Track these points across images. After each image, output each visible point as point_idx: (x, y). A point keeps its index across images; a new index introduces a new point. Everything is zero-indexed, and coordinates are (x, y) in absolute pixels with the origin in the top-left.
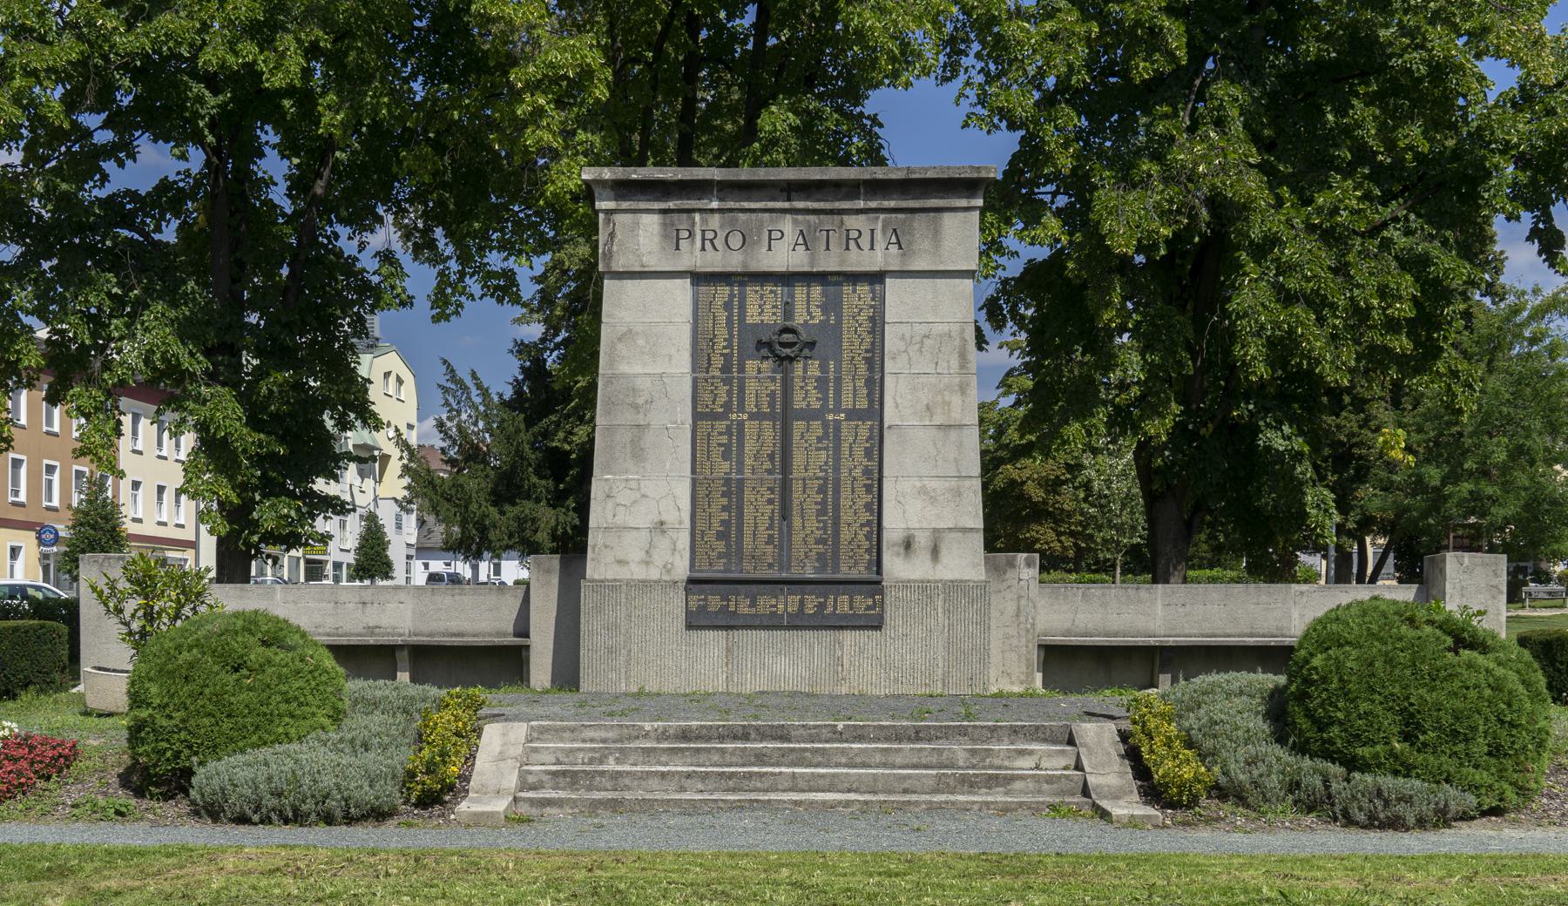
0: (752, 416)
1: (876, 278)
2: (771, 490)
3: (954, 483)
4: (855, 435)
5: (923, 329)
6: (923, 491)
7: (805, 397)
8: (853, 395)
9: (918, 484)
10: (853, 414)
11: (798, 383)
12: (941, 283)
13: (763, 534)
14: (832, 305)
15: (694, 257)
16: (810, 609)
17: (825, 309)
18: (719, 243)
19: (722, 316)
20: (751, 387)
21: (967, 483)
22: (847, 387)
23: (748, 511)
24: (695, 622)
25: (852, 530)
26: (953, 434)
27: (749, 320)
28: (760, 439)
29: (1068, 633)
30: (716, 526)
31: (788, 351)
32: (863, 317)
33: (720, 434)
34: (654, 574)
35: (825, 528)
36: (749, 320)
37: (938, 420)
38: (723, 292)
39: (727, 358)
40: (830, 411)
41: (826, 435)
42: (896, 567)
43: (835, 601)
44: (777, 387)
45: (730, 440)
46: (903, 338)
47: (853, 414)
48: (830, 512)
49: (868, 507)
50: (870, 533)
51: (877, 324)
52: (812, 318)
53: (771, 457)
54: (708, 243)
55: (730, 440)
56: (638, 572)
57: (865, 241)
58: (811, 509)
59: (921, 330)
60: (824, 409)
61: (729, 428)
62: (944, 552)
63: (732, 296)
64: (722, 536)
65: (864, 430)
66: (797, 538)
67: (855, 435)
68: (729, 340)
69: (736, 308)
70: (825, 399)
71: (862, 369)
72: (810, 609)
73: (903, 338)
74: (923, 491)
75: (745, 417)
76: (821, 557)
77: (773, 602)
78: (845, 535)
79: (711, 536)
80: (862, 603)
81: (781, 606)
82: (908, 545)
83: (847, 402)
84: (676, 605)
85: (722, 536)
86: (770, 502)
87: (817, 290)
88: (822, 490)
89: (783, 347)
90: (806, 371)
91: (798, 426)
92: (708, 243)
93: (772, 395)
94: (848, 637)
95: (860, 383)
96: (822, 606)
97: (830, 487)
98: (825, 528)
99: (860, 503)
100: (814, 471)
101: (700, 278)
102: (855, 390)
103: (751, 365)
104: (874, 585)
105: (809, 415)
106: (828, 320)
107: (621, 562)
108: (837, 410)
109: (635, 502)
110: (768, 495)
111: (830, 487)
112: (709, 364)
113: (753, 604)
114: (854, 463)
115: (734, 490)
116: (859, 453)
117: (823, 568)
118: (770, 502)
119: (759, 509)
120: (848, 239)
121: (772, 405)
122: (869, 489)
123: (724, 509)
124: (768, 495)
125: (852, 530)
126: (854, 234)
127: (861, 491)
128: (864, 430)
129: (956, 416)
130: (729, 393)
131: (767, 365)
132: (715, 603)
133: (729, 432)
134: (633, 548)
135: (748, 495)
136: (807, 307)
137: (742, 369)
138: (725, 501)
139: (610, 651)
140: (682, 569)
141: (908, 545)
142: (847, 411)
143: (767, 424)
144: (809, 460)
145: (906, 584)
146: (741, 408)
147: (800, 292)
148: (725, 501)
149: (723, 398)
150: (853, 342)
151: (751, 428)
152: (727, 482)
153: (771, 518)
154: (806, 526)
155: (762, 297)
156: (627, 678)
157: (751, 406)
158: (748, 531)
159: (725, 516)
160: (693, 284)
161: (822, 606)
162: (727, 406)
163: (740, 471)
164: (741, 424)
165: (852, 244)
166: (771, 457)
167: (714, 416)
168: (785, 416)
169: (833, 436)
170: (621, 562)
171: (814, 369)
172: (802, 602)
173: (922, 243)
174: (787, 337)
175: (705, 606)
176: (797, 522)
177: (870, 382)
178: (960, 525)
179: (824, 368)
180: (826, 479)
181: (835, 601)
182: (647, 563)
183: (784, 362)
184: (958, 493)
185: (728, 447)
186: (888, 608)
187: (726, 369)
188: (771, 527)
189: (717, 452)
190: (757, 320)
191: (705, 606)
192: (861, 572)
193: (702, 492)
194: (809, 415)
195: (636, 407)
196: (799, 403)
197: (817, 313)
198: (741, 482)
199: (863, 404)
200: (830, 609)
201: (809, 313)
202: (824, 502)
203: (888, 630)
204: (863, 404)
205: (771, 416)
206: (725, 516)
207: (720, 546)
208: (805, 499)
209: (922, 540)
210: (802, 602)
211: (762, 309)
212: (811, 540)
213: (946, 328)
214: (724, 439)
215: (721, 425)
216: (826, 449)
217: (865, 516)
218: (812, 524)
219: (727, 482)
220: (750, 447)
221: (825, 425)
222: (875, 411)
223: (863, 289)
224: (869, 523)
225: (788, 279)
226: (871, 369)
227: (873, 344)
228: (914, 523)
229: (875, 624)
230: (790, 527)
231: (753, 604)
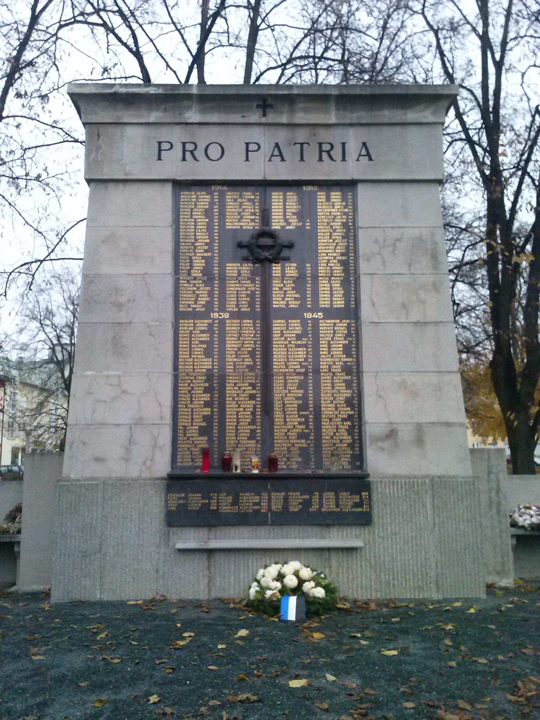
2: (253, 386)
3: (434, 379)
5: (395, 234)
6: (403, 385)
8: (330, 294)
9: (398, 379)
10: (331, 313)
11: (276, 284)
12: (411, 191)
13: (245, 430)
14: (307, 212)
15: (173, 167)
16: (295, 507)
17: (300, 216)
18: (200, 153)
19: (202, 221)
20: (232, 287)
21: (447, 377)
22: (324, 285)
24: (175, 519)
25: (334, 430)
26: (430, 330)
27: (229, 226)
28: (241, 338)
30: (199, 422)
31: (266, 254)
32: (337, 224)
33: (202, 332)
34: (134, 471)
35: (306, 423)
36: (229, 226)
37: (415, 317)
38: (204, 199)
40: (308, 310)
42: (379, 462)
43: (321, 498)
44: (257, 287)
45: (212, 337)
46: (376, 242)
47: (331, 313)
49: (349, 402)
50: (352, 427)
51: (351, 231)
52: (289, 224)
53: (252, 354)
54: (188, 154)
55: (212, 337)
56: (115, 469)
57: (337, 153)
59: (394, 234)
60: (303, 308)
61: (210, 326)
63: (212, 203)
64: (202, 431)
65: (342, 326)
66: (279, 432)
67: (332, 332)
68: (210, 245)
69: (216, 215)
70: (303, 299)
72: (295, 507)
73: (376, 242)
74: (403, 385)
75: (227, 316)
76: (303, 452)
77: (256, 499)
78: (327, 429)
79: (193, 431)
80: (348, 500)
81: (264, 504)
83: (324, 302)
84: (155, 504)
85: (202, 431)
86: (252, 397)
87: (292, 197)
88: (302, 385)
90: (283, 273)
91: (278, 325)
92: (188, 154)
93: (252, 295)
95: (337, 285)
96: (307, 504)
98: (306, 423)
99: (341, 399)
100: (294, 366)
101: (180, 185)
102: (331, 291)
103: (232, 268)
105: (287, 314)
106: (304, 226)
107: (99, 460)
108: (315, 308)
109: (116, 398)
110: (250, 390)
111: (312, 373)
112: (191, 267)
113: (236, 502)
114: (332, 356)
115: (216, 383)
117: (306, 462)
118: (252, 397)
119: (240, 406)
120: (321, 151)
121: (252, 304)
122: (348, 385)
123: (207, 404)
124: (250, 390)
125: (334, 430)
126: (326, 147)
128: (342, 326)
129: (432, 315)
130: (211, 294)
131: (246, 268)
132: (196, 501)
133: (210, 330)
134: (111, 445)
135: (230, 390)
136: (284, 213)
138: (206, 397)
139: (85, 555)
140: (162, 466)
142: (324, 310)
143: (248, 322)
146: (222, 308)
148: (206, 397)
149: (204, 299)
150: (329, 249)
151: (232, 326)
153: (253, 413)
155: (241, 204)
156: (102, 585)
157: (231, 306)
158: (230, 425)
159: (207, 411)
160: (173, 188)
161: (307, 504)
162: (209, 306)
164: (222, 322)
165: (325, 155)
166: (252, 354)
167: (194, 315)
170: (99, 460)
171: (291, 270)
172: (286, 499)
175: (185, 505)
176: (278, 416)
177: (345, 283)
178: (443, 419)
179: (301, 269)
180: (306, 374)
181: (321, 498)
182: (127, 460)
184: (438, 388)
185: (209, 344)
186: (375, 505)
187: (207, 272)
188: (253, 422)
189: (199, 350)
190: (237, 226)
191: (185, 505)
193: (183, 388)
194: (287, 314)
195: (119, 306)
196: (277, 302)
197: (294, 222)
198: (223, 378)
199: (339, 303)
200: (314, 508)
201: (286, 220)
202: (305, 397)
204: (339, 303)
205: (250, 315)
206: (207, 411)
209: (406, 434)
210: (286, 499)
211: (242, 216)
212: (293, 434)
213: (417, 232)
214: (205, 337)
215: (203, 324)
216: (305, 346)
218: (294, 419)
220: (231, 344)
221: (304, 323)
222: (352, 312)
223: (336, 196)
224: (350, 418)
227: (347, 248)
228: (396, 418)
229: (363, 519)
230: (272, 422)
231: (236, 502)
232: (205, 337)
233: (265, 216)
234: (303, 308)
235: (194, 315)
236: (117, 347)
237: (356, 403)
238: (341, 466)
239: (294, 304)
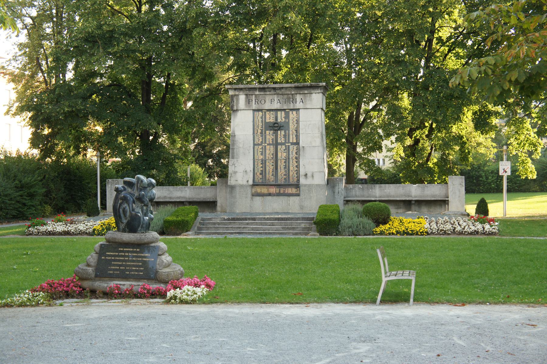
0: (268, 145)
4: (293, 149)
7: (281, 140)
8: (293, 139)
10: (293, 144)
11: (279, 136)
13: (271, 174)
14: (287, 117)
17: (285, 118)
19: (260, 120)
20: (268, 137)
22: (291, 137)
23: (267, 169)
28: (270, 150)
30: (260, 172)
32: (294, 120)
39: (262, 130)
41: (286, 149)
42: (302, 181)
44: (274, 137)
47: (293, 144)
48: (287, 167)
49: (297, 166)
51: (298, 122)
53: (273, 154)
58: (283, 167)
63: (263, 115)
64: (261, 174)
66: (279, 174)
68: (262, 126)
69: (264, 117)
70: (286, 140)
71: (295, 132)
78: (291, 173)
79: (258, 174)
82: (306, 175)
83: (291, 141)
84: (249, 191)
85: (261, 174)
88: (285, 162)
89: (276, 127)
90: (281, 133)
91: (279, 147)
95: (294, 136)
97: (287, 160)
99: (295, 166)
103: (267, 132)
104: (297, 186)
105: (282, 144)
108: (289, 142)
111: (287, 160)
114: (293, 155)
115: (264, 162)
116: (294, 153)
118: (273, 165)
119: (270, 167)
121: (273, 141)
122: (297, 162)
123: (262, 167)
128: (295, 147)
130: (262, 139)
131: (272, 132)
133: (262, 148)
135: (267, 164)
136: (281, 117)
137: (265, 133)
138: (261, 165)
141: (306, 175)
144: (282, 155)
145: (305, 185)
146: (265, 143)
147: (279, 113)
148: (261, 165)
149: (261, 140)
150: (292, 126)
151: (268, 147)
152: (262, 160)
154: (281, 172)
157: (267, 142)
158: (267, 172)
159: (262, 169)
161: (284, 191)
162: (262, 142)
163: (265, 158)
164: (265, 146)
166: (273, 154)
167: (258, 145)
168: (276, 144)
169: (288, 149)
171: (283, 133)
173: (308, 102)
174: (276, 125)
177: (296, 136)
179: (285, 132)
185: (262, 152)
187: (261, 133)
189: (259, 153)
190: (269, 121)
194: (282, 144)
196: (279, 141)
197: (284, 119)
199: (295, 141)
203: (301, 197)
204: (295, 141)
205: (273, 144)
206: (262, 169)
207: (261, 176)
208: (281, 164)
209: (309, 175)
211: (270, 118)
212: (283, 175)
214: (261, 150)
215: (260, 147)
217: (296, 169)
218: (283, 171)
219: (262, 160)
220: (268, 152)
221: (286, 146)
222: (297, 143)
223: (294, 112)
224: (297, 170)
226: (297, 132)
229: (298, 195)
232: (261, 150)
233: (276, 118)
234: (285, 142)
235: (258, 145)
237: (298, 166)
238: (293, 180)
239: (283, 141)
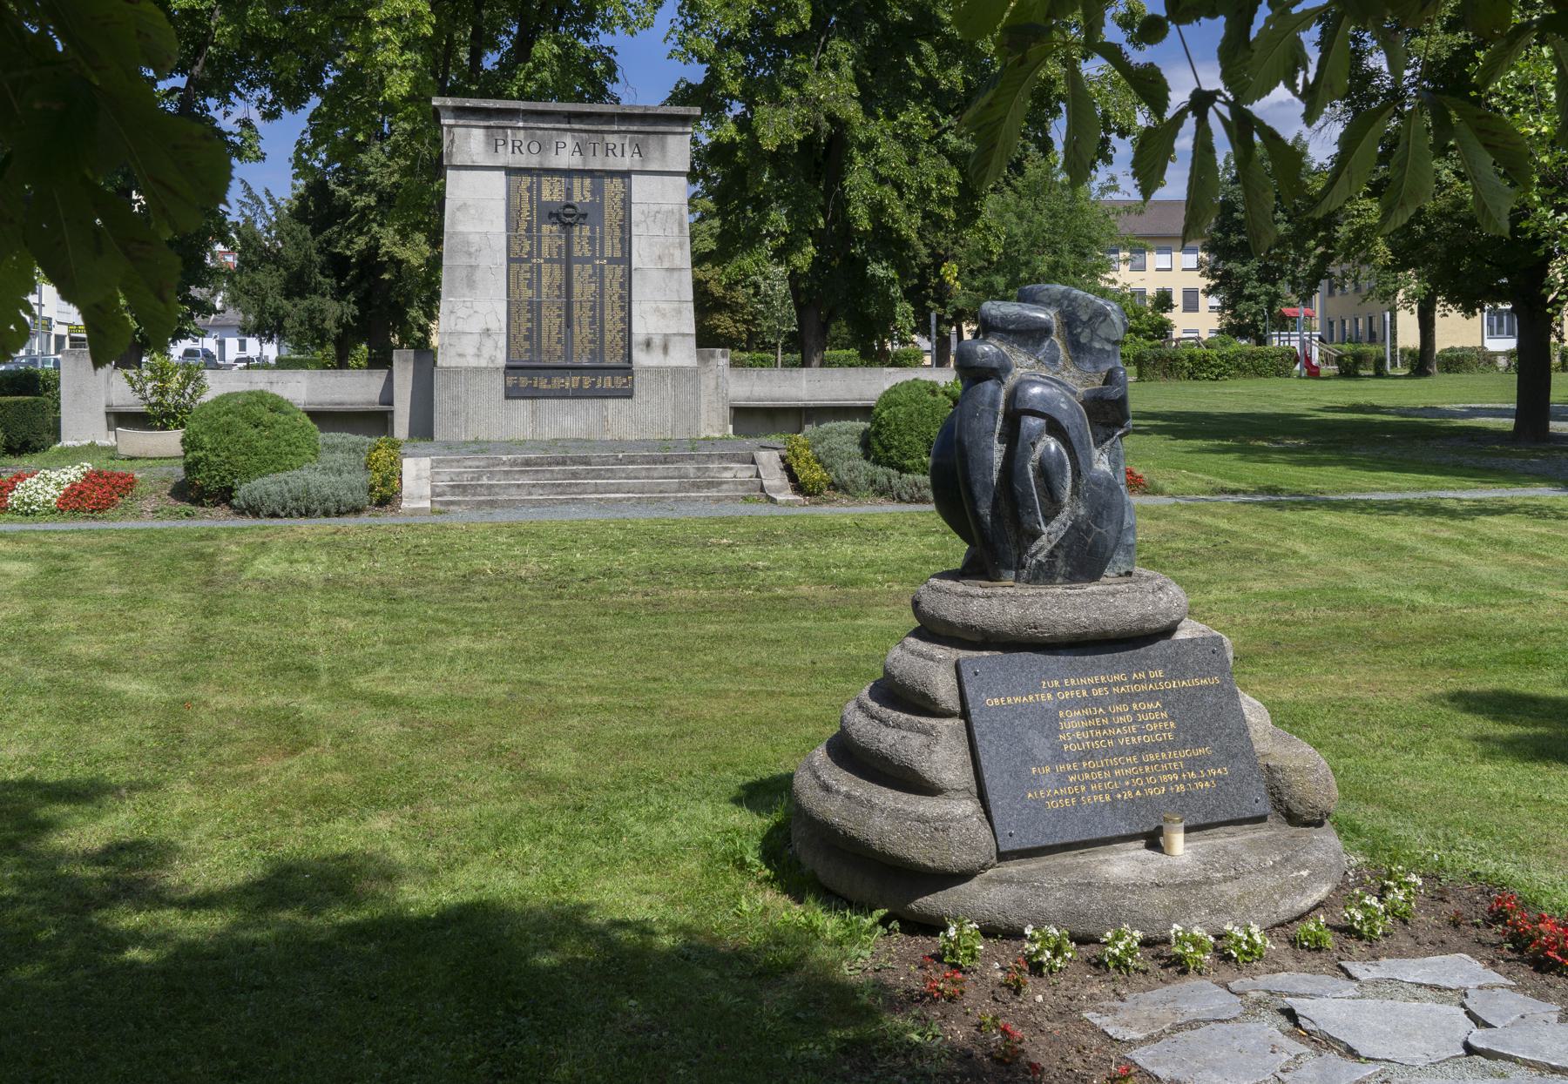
0: (546, 261)
1: (626, 175)
3: (676, 305)
4: (614, 274)
5: (656, 208)
6: (657, 310)
7: (581, 249)
8: (611, 248)
10: (612, 261)
11: (576, 240)
12: (666, 178)
14: (597, 191)
15: (506, 157)
16: (586, 385)
17: (593, 193)
20: (546, 243)
22: (608, 243)
23: (544, 323)
24: (511, 394)
26: (676, 274)
28: (551, 276)
29: (748, 399)
30: (524, 332)
34: (483, 363)
38: (527, 180)
39: (530, 223)
41: (594, 274)
42: (640, 358)
47: (612, 261)
48: (598, 322)
49: (622, 320)
51: (627, 203)
53: (559, 287)
56: (472, 362)
57: (618, 151)
58: (586, 321)
60: (593, 257)
62: (671, 348)
64: (527, 338)
65: (619, 271)
66: (577, 339)
67: (614, 274)
68: (531, 211)
70: (594, 251)
71: (618, 232)
72: (586, 385)
74: (657, 310)
76: (592, 352)
78: (608, 337)
79: (520, 338)
80: (620, 381)
82: (648, 344)
83: (608, 253)
84: (499, 383)
85: (527, 338)
87: (587, 181)
88: (593, 309)
89: (566, 217)
90: (581, 233)
91: (576, 268)
94: (611, 403)
95: (616, 241)
96: (594, 384)
97: (597, 307)
101: (510, 171)
103: (546, 228)
104: (627, 369)
105: (584, 260)
107: (461, 355)
108: (601, 258)
113: (549, 382)
114: (613, 289)
115: (535, 308)
116: (616, 286)
117: (593, 359)
119: (551, 321)
121: (559, 254)
122: (622, 308)
127: (617, 309)
129: (678, 263)
132: (524, 381)
133: (531, 270)
134: (468, 346)
136: (582, 192)
137: (539, 230)
139: (454, 413)
140: (501, 360)
141: (648, 344)
143: (556, 266)
144: (583, 289)
145: (647, 369)
146: (539, 256)
147: (577, 182)
149: (527, 248)
150: (611, 214)
151: (545, 268)
152: (531, 303)
154: (582, 331)
162: (530, 253)
163: (539, 296)
164: (539, 266)
166: (559, 287)
167: (521, 260)
168: (568, 261)
169: (599, 275)
170: (461, 355)
171: (586, 231)
173: (654, 153)
174: (569, 210)
176: (576, 329)
177: (622, 240)
179: (593, 231)
183: (567, 226)
184: (679, 312)
185: (530, 280)
187: (529, 230)
189: (523, 284)
192: (617, 361)
193: (514, 309)
194: (584, 260)
195: (470, 254)
196: (577, 252)
197: (588, 195)
198: (540, 303)
199: (618, 254)
203: (636, 398)
204: (618, 254)
205: (559, 261)
207: (527, 345)
208: (582, 315)
209: (657, 341)
211: (552, 192)
214: (528, 275)
215: (526, 266)
217: (620, 326)
218: (586, 331)
219: (531, 303)
220: (545, 280)
221: (594, 266)
222: (626, 259)
223: (617, 181)
225: (569, 173)
226: (623, 231)
229: (628, 394)
231: (549, 382)
232: (528, 275)
233: (569, 192)
234: (593, 257)
235: (521, 260)
236: (471, 283)
237: (628, 320)
239: (588, 254)
